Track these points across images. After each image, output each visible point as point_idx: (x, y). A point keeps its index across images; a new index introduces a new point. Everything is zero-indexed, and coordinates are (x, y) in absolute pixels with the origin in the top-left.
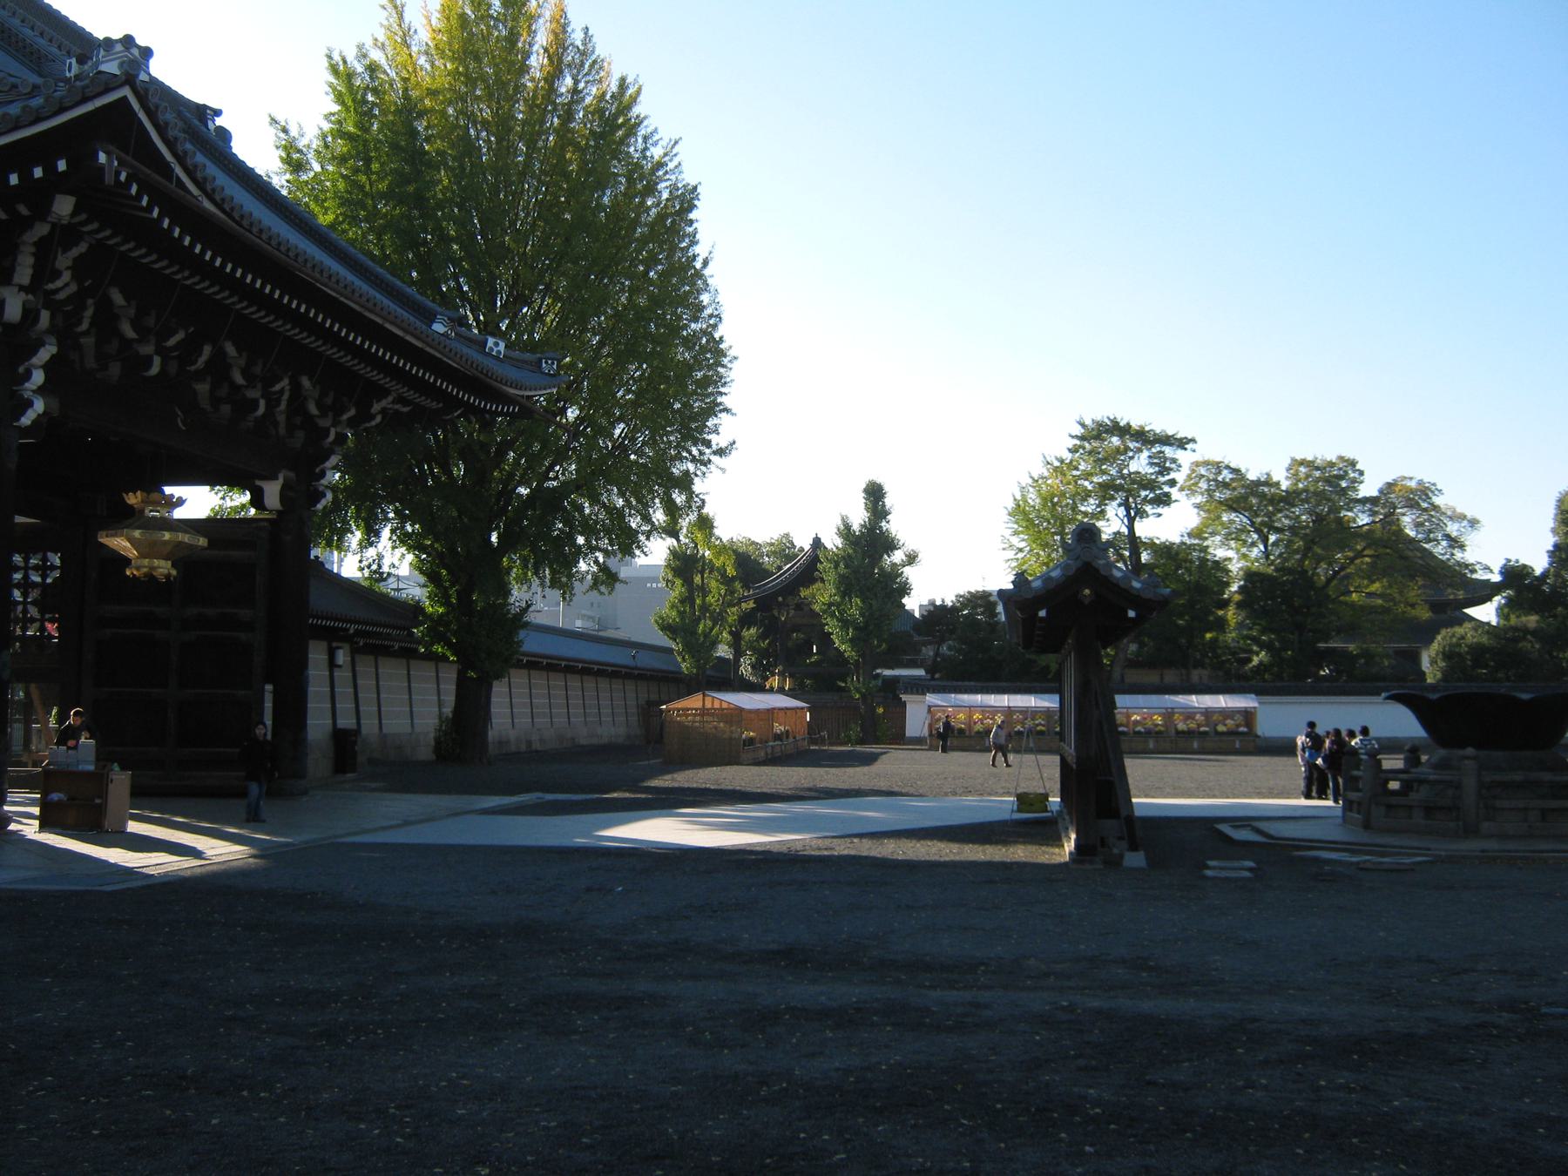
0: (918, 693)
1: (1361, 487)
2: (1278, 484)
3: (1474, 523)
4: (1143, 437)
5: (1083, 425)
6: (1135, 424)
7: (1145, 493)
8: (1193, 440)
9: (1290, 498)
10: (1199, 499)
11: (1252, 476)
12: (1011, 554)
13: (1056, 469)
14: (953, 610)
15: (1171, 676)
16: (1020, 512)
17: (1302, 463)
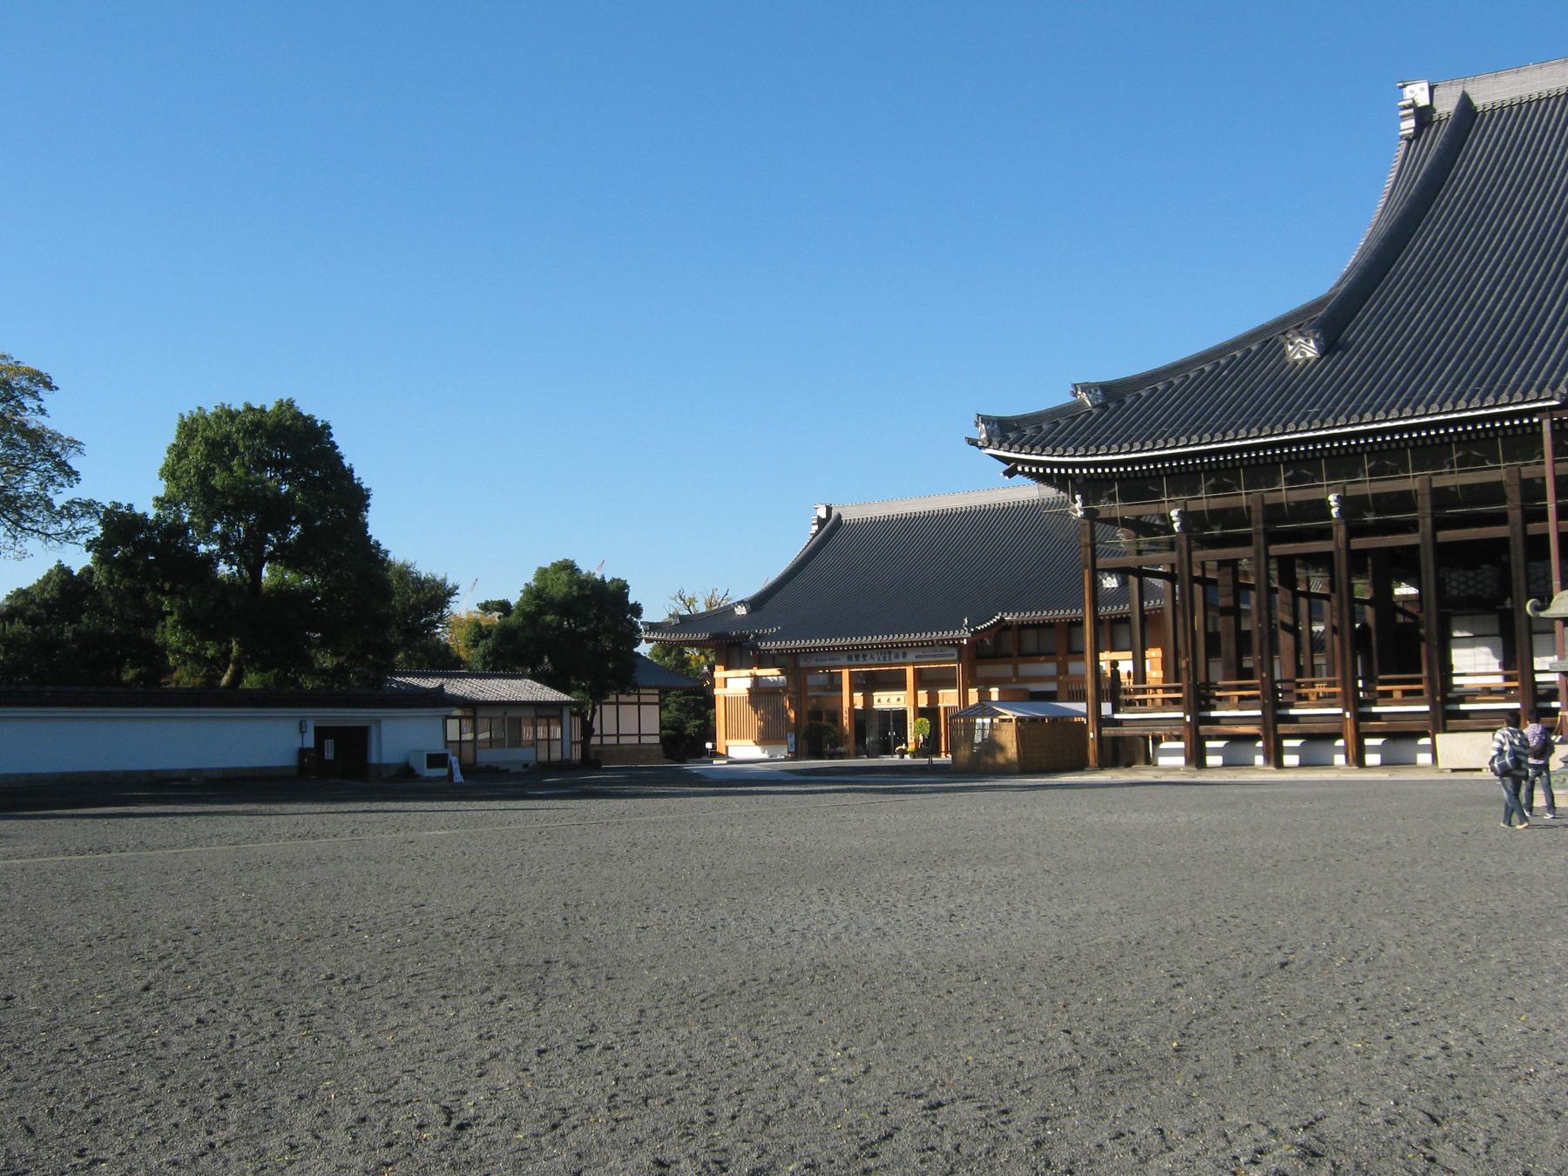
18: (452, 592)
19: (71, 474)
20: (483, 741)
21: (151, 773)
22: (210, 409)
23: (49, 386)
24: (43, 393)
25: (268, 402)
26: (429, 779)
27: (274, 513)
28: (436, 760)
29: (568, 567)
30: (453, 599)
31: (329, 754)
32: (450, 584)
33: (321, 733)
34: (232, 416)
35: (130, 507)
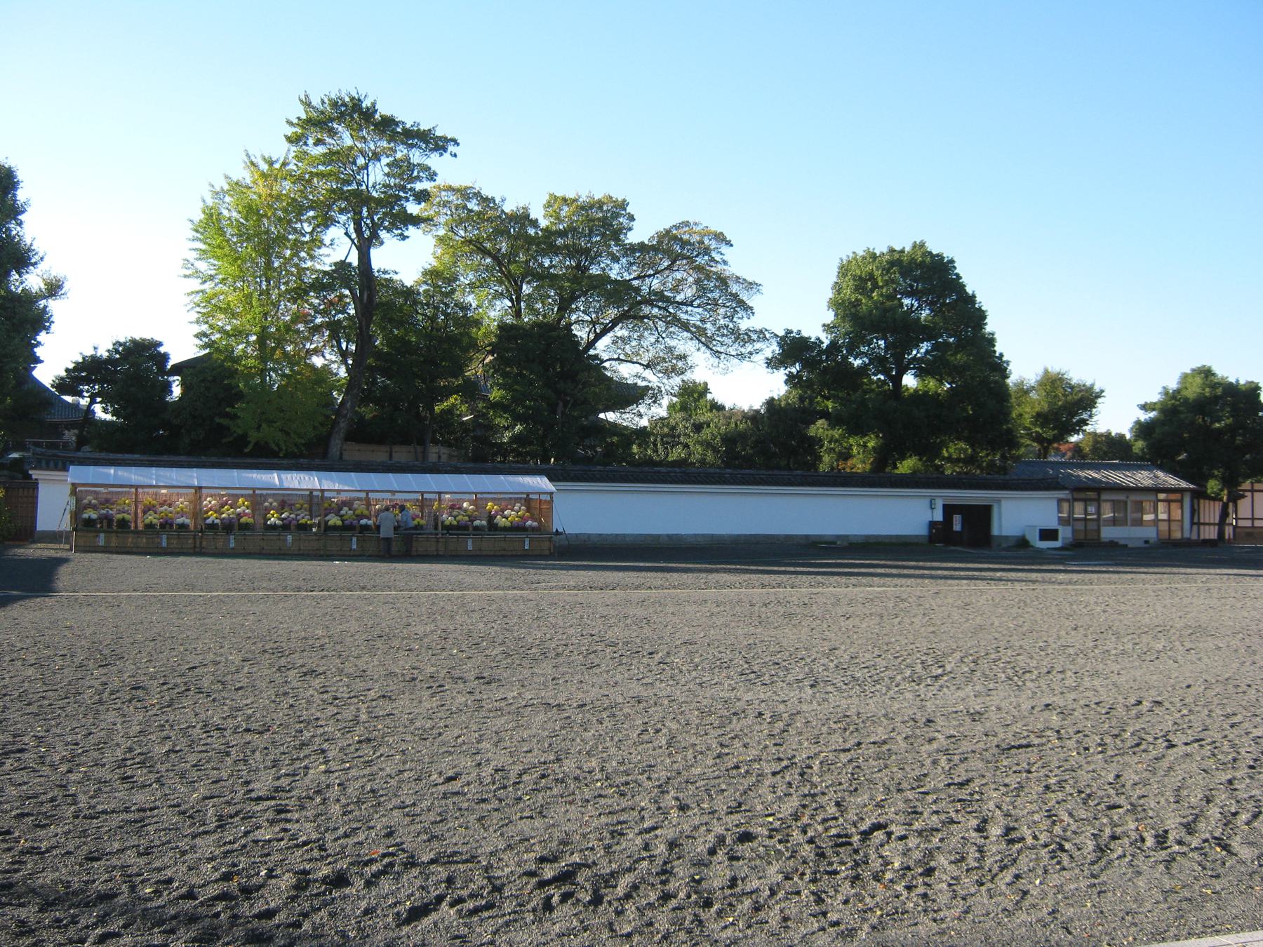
0: (56, 468)
1: (629, 234)
2: (534, 223)
3: (751, 286)
4: (387, 126)
5: (307, 104)
6: (384, 110)
7: (381, 214)
8: (456, 143)
9: (547, 242)
10: (442, 232)
11: (508, 208)
12: (195, 284)
13: (264, 175)
14: (109, 360)
15: (402, 454)
16: (211, 223)
17: (565, 200)
18: (1098, 396)
19: (748, 309)
20: (1106, 520)
21: (807, 536)
22: (861, 253)
23: (729, 243)
24: (724, 249)
25: (904, 243)
26: (1041, 551)
27: (904, 332)
28: (1048, 534)
29: (1206, 373)
30: (1099, 400)
31: (957, 526)
32: (1097, 389)
33: (949, 510)
34: (874, 256)
35: (799, 332)
